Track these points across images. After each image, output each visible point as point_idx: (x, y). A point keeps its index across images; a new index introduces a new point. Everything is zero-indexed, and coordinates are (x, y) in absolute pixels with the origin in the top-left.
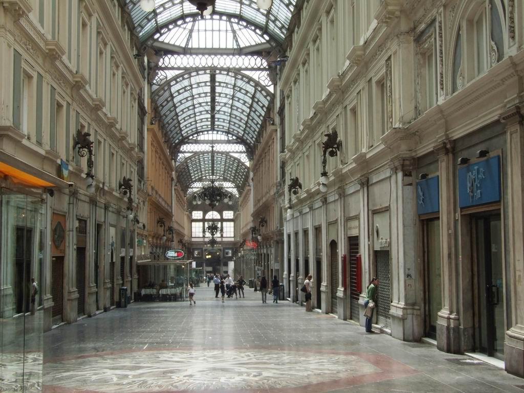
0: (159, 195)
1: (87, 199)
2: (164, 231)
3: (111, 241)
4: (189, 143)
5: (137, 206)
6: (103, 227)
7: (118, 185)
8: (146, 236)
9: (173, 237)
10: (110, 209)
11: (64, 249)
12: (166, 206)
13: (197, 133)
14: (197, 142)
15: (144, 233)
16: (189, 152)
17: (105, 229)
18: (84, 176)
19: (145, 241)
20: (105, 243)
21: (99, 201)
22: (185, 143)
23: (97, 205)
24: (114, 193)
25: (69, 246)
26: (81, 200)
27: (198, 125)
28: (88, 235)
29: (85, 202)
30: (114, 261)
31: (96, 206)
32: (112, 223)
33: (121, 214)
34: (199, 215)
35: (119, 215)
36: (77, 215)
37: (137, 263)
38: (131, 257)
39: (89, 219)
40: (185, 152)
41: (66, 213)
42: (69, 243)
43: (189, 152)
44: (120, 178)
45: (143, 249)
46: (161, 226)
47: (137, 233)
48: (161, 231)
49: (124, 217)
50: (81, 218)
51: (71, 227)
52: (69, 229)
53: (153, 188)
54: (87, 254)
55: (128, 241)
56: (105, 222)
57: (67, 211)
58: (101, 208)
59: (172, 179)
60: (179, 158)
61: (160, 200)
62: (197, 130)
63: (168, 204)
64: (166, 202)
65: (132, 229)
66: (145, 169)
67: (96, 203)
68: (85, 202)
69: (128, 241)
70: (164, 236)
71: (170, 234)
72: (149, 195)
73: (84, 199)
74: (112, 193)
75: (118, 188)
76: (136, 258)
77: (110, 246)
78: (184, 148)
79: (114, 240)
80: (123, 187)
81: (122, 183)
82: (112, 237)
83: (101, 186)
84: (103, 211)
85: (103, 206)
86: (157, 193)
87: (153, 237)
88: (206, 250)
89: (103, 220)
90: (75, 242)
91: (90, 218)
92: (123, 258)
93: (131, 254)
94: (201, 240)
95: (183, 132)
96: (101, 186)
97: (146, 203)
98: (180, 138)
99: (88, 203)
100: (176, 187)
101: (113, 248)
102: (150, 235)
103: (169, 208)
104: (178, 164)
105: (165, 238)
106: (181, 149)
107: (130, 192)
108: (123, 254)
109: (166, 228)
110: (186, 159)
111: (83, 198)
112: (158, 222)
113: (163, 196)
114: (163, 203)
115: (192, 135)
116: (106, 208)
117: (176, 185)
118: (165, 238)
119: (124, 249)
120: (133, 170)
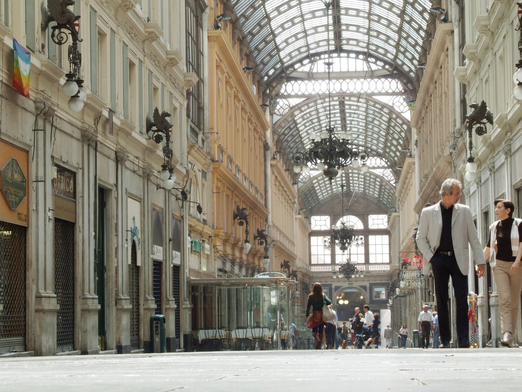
0: (237, 166)
1: (77, 134)
2: (247, 232)
3: (130, 225)
4: (296, 79)
5: (187, 171)
6: (114, 194)
7: (144, 123)
8: (210, 237)
9: (266, 249)
10: (127, 163)
11: (25, 213)
12: (252, 191)
13: (312, 57)
14: (310, 76)
15: (205, 230)
16: (297, 96)
17: (117, 199)
18: (63, 81)
19: (207, 246)
20: (117, 224)
21: (101, 143)
22: (289, 79)
23: (99, 149)
24: (135, 135)
25: (37, 210)
26: (61, 131)
27: (311, 39)
28: (79, 200)
29: (72, 136)
30: (139, 264)
31: (96, 150)
32: (134, 192)
33: (152, 178)
34: (323, 223)
35: (148, 179)
36: (52, 157)
37: (189, 282)
38: (177, 269)
39: (80, 171)
40: (289, 96)
41: (30, 147)
42: (37, 205)
43: (297, 96)
44: (147, 113)
45: (204, 261)
46: (241, 224)
47: (190, 226)
48: (240, 231)
49: (158, 187)
50: (62, 164)
51: (41, 174)
52: (37, 177)
53: (221, 150)
54: (79, 237)
55: (168, 233)
56: (116, 185)
57: (32, 143)
58: (109, 158)
59: (266, 147)
60: (278, 107)
61: (239, 176)
62: (309, 49)
63: (256, 188)
64: (251, 184)
65: (178, 214)
66: (207, 113)
67: (96, 144)
68: (72, 136)
69: (168, 233)
70: (247, 241)
71: (261, 243)
72: (213, 160)
73: (69, 132)
74: (130, 134)
75: (144, 130)
76: (187, 271)
77: (129, 233)
78: (288, 88)
79: (138, 224)
80: (154, 128)
81: (152, 120)
82: (134, 219)
83: (106, 113)
84: (112, 164)
85: (113, 156)
86: (231, 161)
87: (225, 242)
88: (337, 288)
89: (112, 180)
90: (50, 204)
91: (83, 169)
92: (158, 265)
93: (177, 261)
94: (329, 269)
95: (282, 54)
96: (106, 113)
97: (209, 176)
98: (278, 66)
99: (78, 140)
100: (274, 162)
101: (135, 238)
102: (217, 236)
103: (258, 197)
104: (276, 118)
105: (248, 246)
106: (282, 91)
107: (168, 137)
108: (159, 255)
109: (253, 232)
110: (292, 109)
111: (68, 129)
112: (235, 217)
113: (245, 171)
114: (246, 184)
115: (301, 61)
116: (119, 159)
117: (274, 158)
118: (248, 246)
119: (161, 248)
120: (177, 105)
